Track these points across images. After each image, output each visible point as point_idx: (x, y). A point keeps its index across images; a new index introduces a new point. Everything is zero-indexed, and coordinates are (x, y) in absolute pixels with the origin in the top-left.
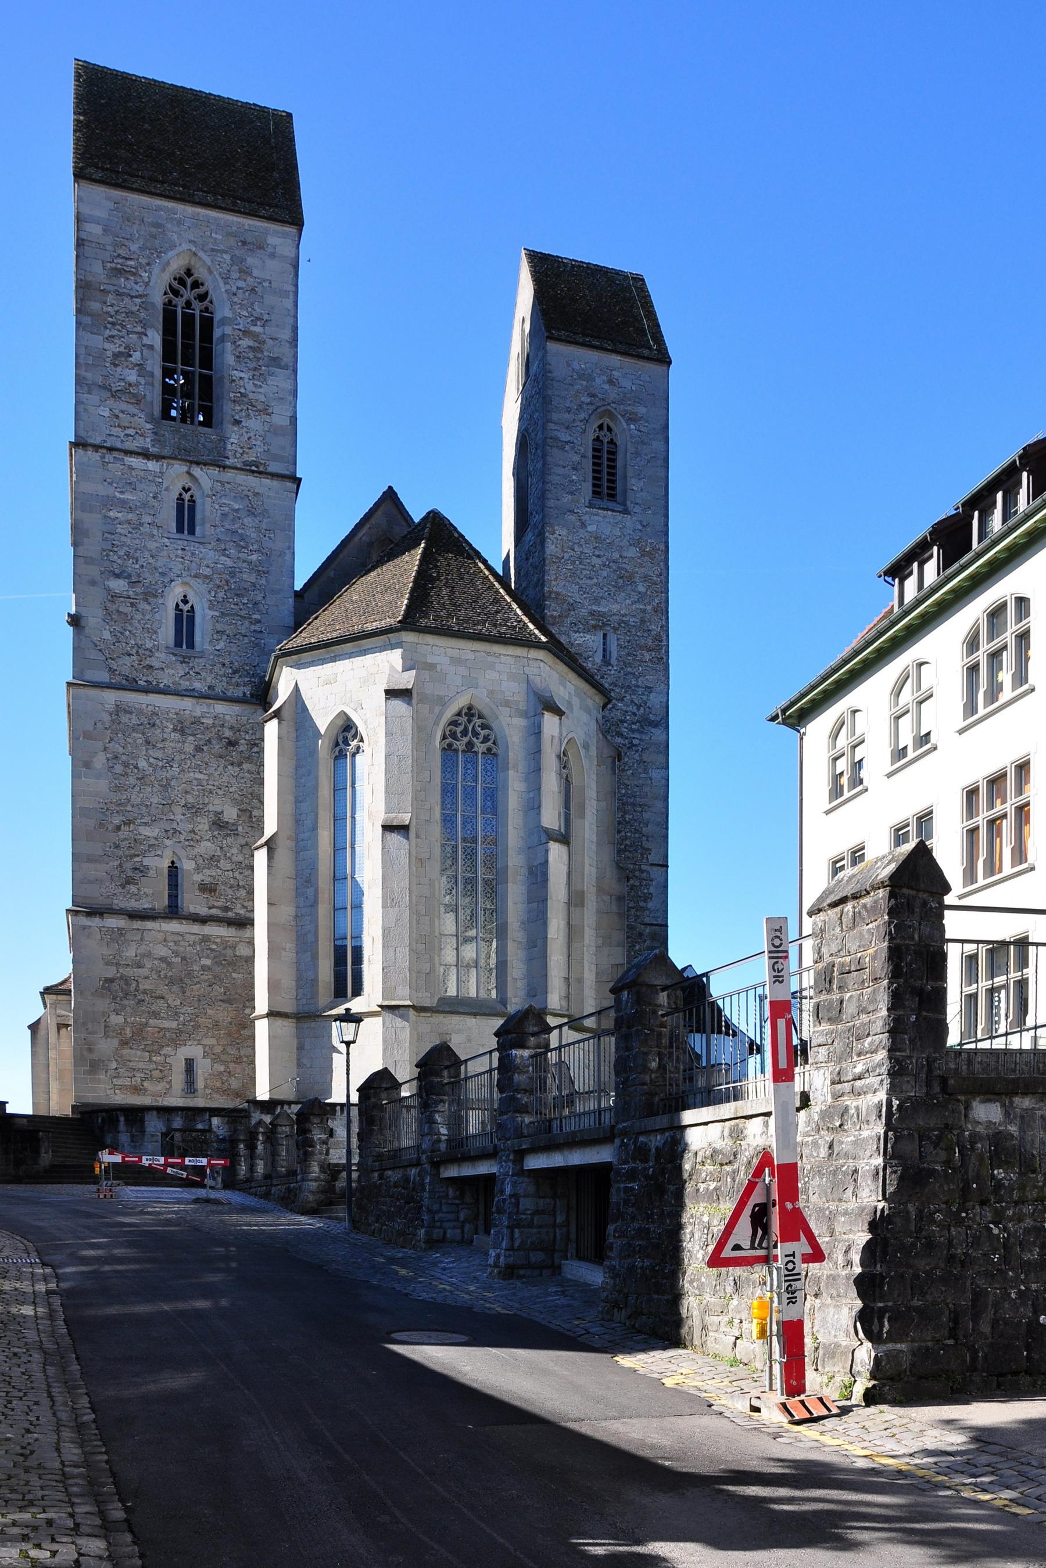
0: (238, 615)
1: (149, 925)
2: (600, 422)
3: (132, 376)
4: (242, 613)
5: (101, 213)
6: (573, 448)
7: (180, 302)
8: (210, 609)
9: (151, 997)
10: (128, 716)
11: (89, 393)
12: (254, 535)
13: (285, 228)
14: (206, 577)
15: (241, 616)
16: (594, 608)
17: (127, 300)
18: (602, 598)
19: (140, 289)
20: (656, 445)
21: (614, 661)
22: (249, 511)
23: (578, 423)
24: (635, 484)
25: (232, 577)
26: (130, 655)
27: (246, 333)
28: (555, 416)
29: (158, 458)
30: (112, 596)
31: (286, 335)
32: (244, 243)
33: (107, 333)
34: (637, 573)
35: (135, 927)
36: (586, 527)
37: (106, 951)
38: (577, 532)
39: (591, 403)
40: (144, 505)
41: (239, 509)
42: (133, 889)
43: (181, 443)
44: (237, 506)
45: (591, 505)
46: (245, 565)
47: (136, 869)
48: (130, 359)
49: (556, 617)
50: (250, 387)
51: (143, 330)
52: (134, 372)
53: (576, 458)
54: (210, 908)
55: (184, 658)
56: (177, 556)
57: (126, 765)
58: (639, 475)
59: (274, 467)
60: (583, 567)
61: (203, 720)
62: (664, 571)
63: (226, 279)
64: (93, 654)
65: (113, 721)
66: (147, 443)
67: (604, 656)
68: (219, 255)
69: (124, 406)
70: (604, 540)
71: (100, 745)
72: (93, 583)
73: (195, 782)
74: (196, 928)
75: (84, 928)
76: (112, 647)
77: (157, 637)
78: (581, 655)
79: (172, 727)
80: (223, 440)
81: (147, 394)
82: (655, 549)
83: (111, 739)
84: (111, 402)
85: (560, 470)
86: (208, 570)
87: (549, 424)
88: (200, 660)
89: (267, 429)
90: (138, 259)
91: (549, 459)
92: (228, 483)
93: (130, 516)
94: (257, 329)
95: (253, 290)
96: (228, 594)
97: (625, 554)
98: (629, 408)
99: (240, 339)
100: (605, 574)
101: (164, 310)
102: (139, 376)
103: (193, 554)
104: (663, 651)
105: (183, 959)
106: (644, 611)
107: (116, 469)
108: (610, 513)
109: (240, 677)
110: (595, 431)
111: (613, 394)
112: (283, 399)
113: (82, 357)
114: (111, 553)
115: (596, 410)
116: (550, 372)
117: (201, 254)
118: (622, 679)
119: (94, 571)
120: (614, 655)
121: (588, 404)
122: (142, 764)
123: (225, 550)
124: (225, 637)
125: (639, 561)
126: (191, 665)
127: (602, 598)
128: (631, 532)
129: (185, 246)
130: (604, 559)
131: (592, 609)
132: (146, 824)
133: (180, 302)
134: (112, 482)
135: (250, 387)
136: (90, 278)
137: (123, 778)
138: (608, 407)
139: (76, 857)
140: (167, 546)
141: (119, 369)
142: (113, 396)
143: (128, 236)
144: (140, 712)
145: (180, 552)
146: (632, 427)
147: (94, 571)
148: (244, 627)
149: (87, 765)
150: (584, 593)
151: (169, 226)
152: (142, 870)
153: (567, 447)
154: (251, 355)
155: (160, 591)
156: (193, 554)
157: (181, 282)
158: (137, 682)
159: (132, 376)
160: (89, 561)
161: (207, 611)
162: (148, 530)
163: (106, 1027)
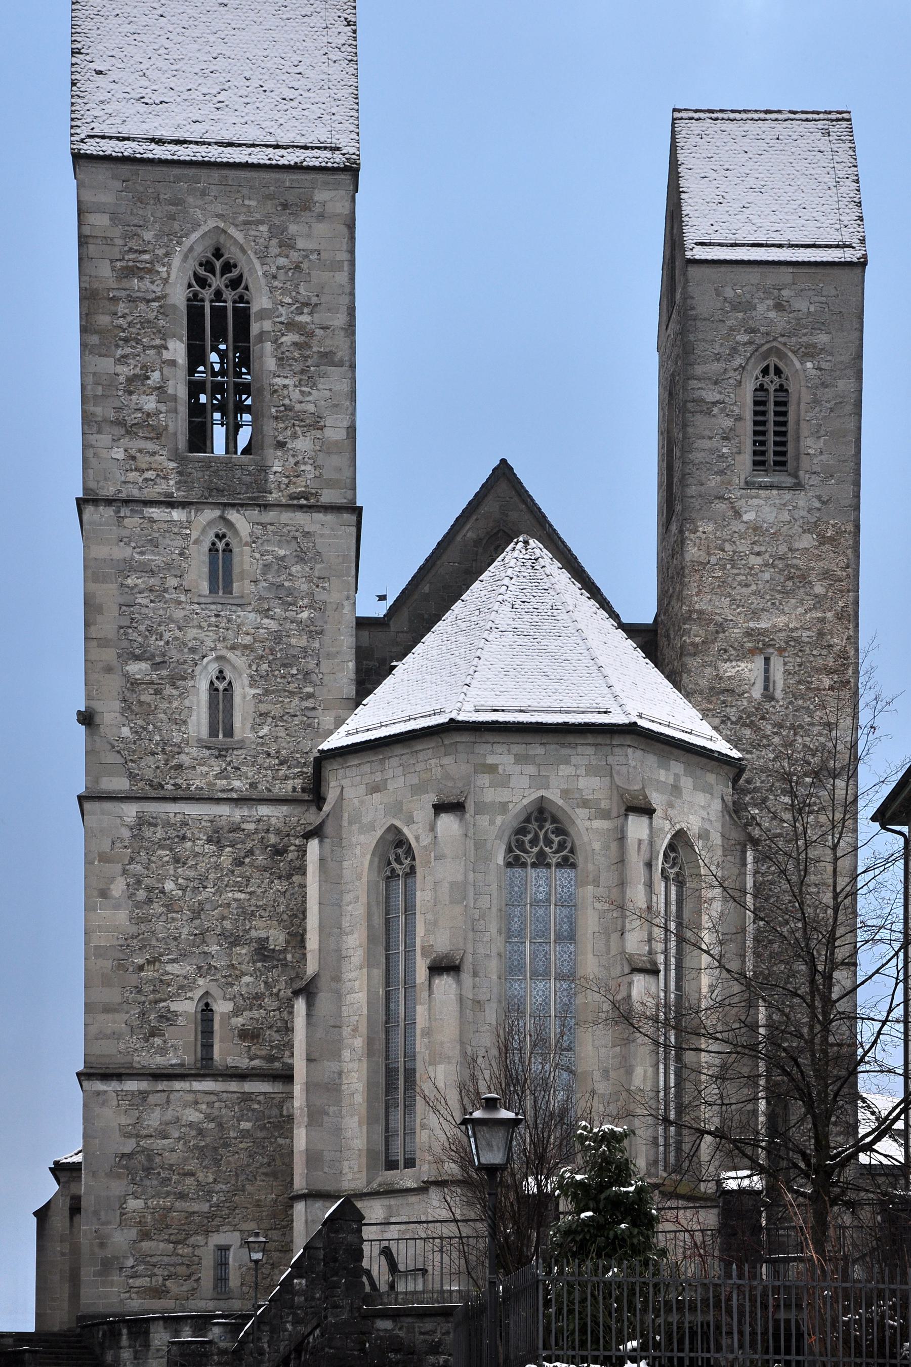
0: (285, 691)
1: (178, 1085)
2: (765, 364)
3: (150, 403)
4: (291, 687)
5: (106, 198)
6: (722, 410)
8: (251, 686)
9: (179, 1174)
10: (152, 829)
11: (99, 432)
12: (304, 587)
13: (336, 177)
14: (246, 647)
15: (288, 691)
16: (751, 624)
17: (142, 306)
18: (763, 610)
19: (158, 289)
20: (844, 385)
21: (779, 694)
22: (298, 557)
23: (731, 374)
24: (810, 445)
25: (279, 643)
26: (153, 754)
27: (291, 326)
28: (699, 370)
29: (183, 505)
30: (132, 684)
31: (340, 320)
32: (285, 206)
33: (119, 352)
34: (813, 569)
35: (160, 1088)
36: (741, 516)
37: (124, 1120)
38: (729, 524)
39: (750, 343)
40: (169, 566)
41: (285, 556)
42: (158, 1041)
43: (211, 481)
44: (282, 552)
45: (749, 485)
46: (294, 626)
47: (161, 1017)
48: (149, 382)
49: (697, 644)
50: (296, 395)
51: (163, 342)
52: (153, 398)
53: (728, 423)
54: (251, 1059)
55: (220, 750)
56: (209, 626)
57: (150, 889)
58: (818, 431)
59: (328, 496)
60: (736, 571)
61: (244, 826)
62: (852, 562)
63: (263, 258)
64: (112, 758)
65: (133, 836)
66: (170, 486)
67: (766, 688)
68: (254, 227)
69: (142, 444)
70: (767, 530)
71: (119, 867)
72: (109, 669)
73: (234, 905)
74: (233, 1086)
75: (98, 1093)
76: (133, 746)
77: (187, 728)
78: (733, 691)
79: (205, 838)
80: (264, 469)
81: (170, 423)
82: (839, 533)
83: (132, 859)
84: (125, 441)
85: (706, 444)
86: (249, 638)
87: (690, 382)
88: (240, 752)
89: (318, 448)
90: (154, 251)
91: (690, 430)
92: (271, 524)
93: (152, 581)
94: (304, 318)
95: (297, 268)
96: (274, 666)
97: (796, 545)
98: (805, 339)
99: (283, 335)
100: (767, 576)
102: (159, 402)
103: (229, 621)
104: (850, 671)
105: (220, 1125)
106: (822, 620)
107: (133, 522)
108: (775, 492)
109: (289, 768)
110: (757, 378)
111: (780, 322)
112: (336, 406)
113: (89, 387)
114: (130, 631)
115: (756, 351)
116: (693, 308)
117: (232, 231)
118: (790, 717)
119: (109, 655)
120: (780, 685)
121: (745, 344)
122: (169, 886)
123: (269, 610)
124: (270, 719)
125: (817, 552)
126: (228, 759)
127: (763, 610)
128: (805, 513)
129: (212, 223)
130: (767, 556)
131: (748, 628)
132: (173, 961)
134: (130, 541)
135: (296, 395)
137: (146, 907)
138: (774, 344)
139: (89, 1008)
140: (197, 614)
141: (134, 397)
142: (128, 432)
143: (141, 223)
144: (167, 824)
145: (213, 619)
146: (809, 365)
147: (109, 655)
148: (293, 704)
149: (104, 894)
150: (738, 606)
151: (190, 200)
152: (168, 1017)
153: (716, 410)
154: (296, 355)
155: (190, 671)
156: (229, 621)
158: (163, 787)
159: (150, 403)
160: (103, 643)
161: (247, 689)
162: (174, 596)
163: (122, 1214)
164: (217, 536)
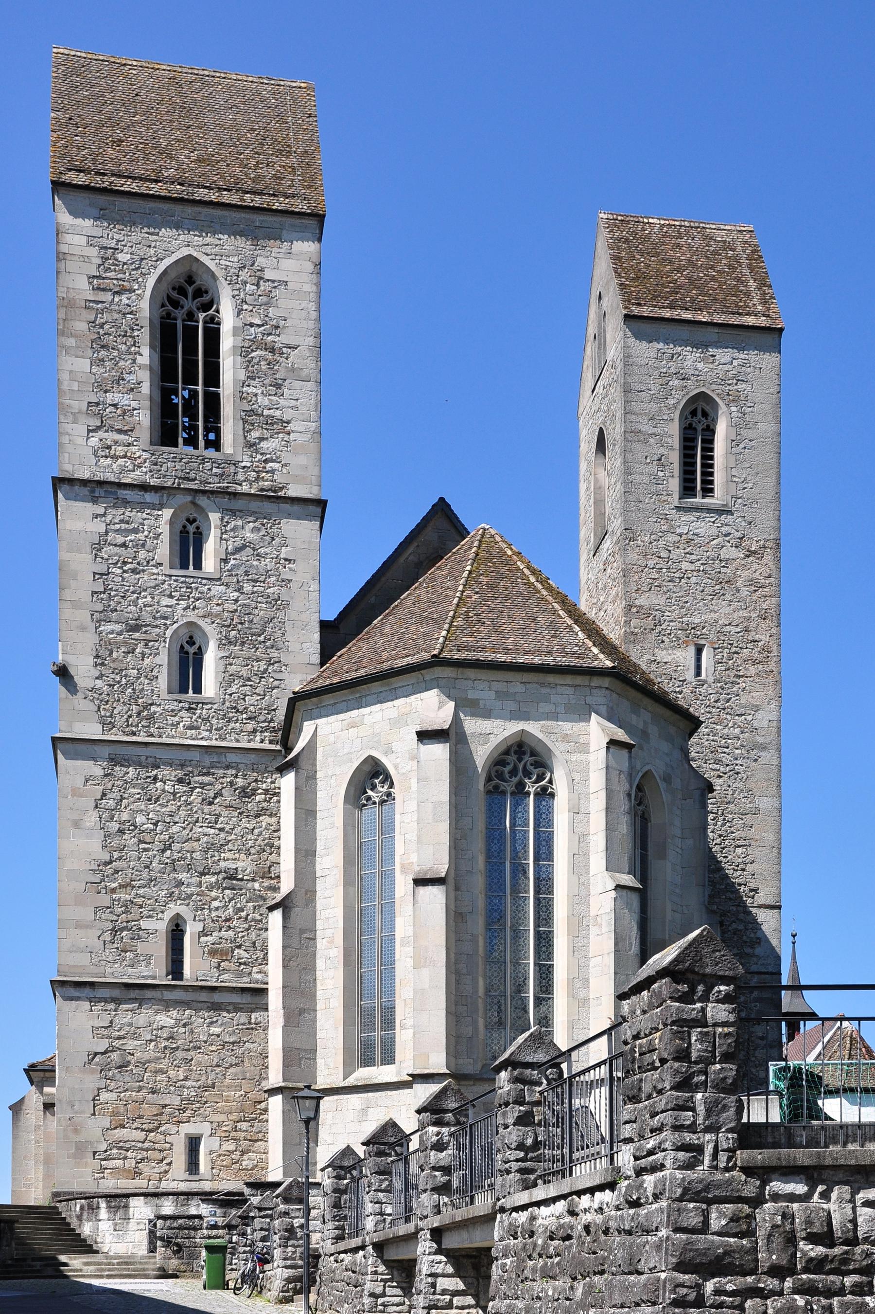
7: (180, 314)
101: (162, 324)
133: (180, 314)
136: (72, 294)
157: (182, 291)
164: (188, 520)
